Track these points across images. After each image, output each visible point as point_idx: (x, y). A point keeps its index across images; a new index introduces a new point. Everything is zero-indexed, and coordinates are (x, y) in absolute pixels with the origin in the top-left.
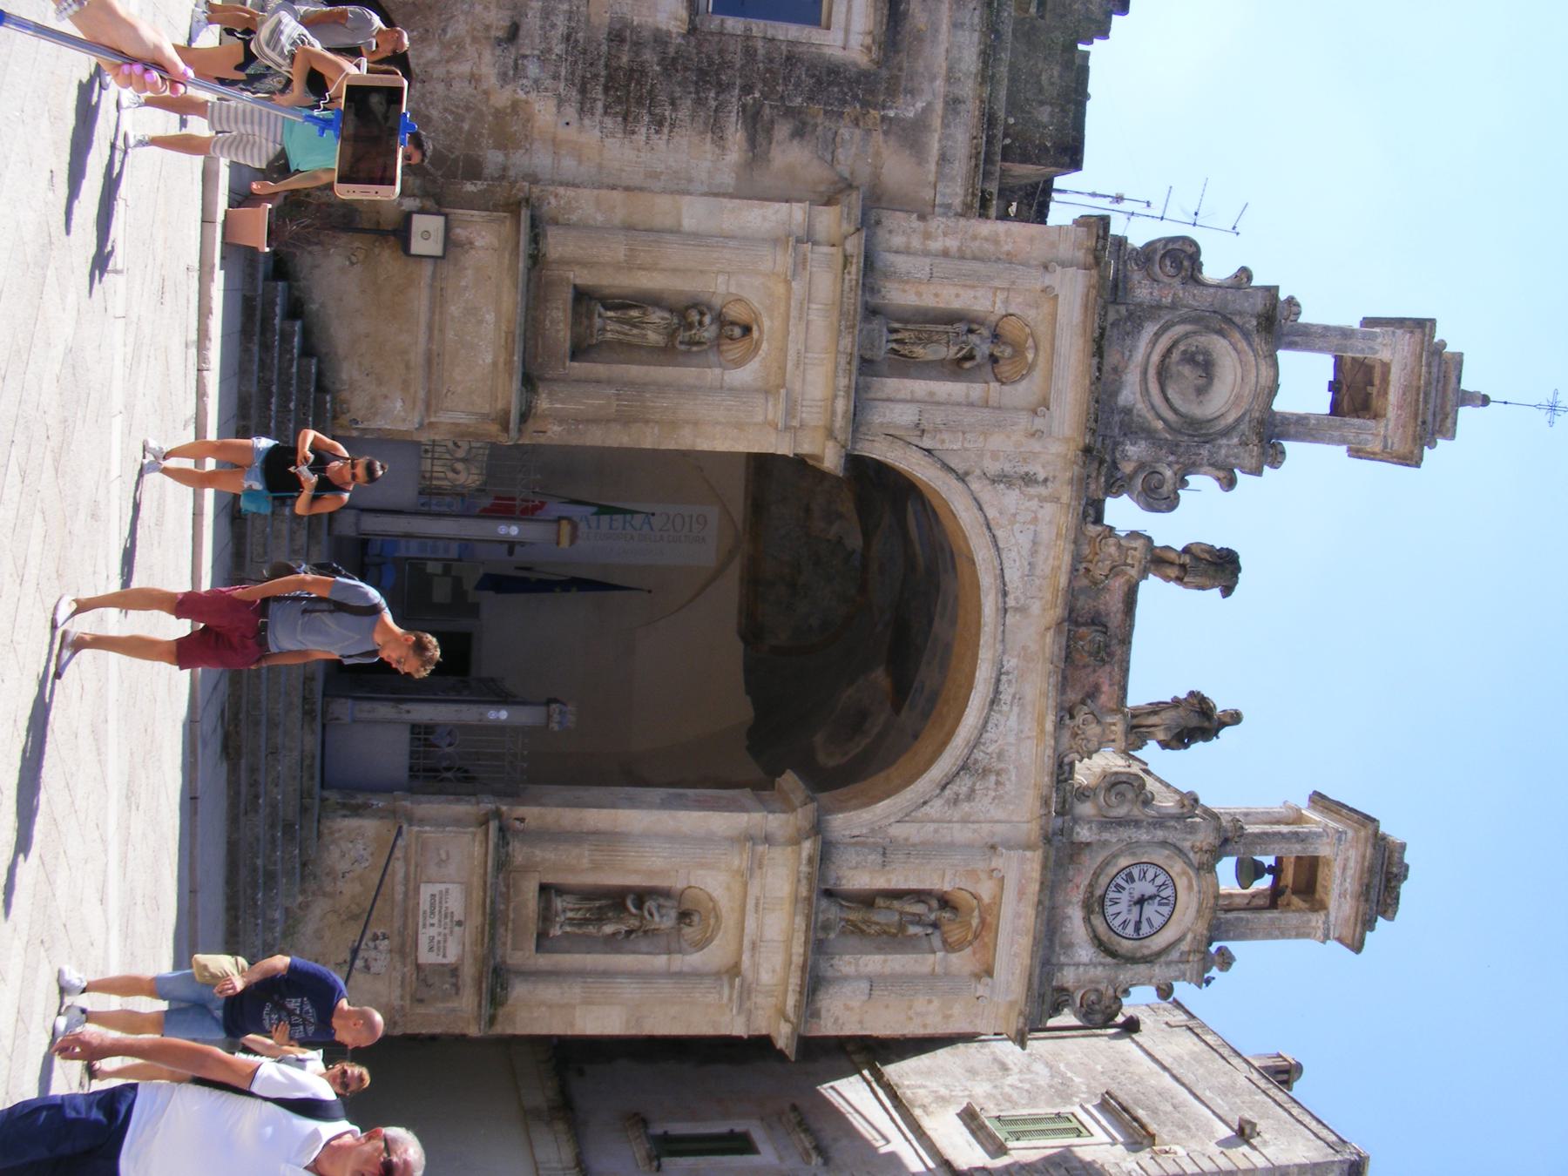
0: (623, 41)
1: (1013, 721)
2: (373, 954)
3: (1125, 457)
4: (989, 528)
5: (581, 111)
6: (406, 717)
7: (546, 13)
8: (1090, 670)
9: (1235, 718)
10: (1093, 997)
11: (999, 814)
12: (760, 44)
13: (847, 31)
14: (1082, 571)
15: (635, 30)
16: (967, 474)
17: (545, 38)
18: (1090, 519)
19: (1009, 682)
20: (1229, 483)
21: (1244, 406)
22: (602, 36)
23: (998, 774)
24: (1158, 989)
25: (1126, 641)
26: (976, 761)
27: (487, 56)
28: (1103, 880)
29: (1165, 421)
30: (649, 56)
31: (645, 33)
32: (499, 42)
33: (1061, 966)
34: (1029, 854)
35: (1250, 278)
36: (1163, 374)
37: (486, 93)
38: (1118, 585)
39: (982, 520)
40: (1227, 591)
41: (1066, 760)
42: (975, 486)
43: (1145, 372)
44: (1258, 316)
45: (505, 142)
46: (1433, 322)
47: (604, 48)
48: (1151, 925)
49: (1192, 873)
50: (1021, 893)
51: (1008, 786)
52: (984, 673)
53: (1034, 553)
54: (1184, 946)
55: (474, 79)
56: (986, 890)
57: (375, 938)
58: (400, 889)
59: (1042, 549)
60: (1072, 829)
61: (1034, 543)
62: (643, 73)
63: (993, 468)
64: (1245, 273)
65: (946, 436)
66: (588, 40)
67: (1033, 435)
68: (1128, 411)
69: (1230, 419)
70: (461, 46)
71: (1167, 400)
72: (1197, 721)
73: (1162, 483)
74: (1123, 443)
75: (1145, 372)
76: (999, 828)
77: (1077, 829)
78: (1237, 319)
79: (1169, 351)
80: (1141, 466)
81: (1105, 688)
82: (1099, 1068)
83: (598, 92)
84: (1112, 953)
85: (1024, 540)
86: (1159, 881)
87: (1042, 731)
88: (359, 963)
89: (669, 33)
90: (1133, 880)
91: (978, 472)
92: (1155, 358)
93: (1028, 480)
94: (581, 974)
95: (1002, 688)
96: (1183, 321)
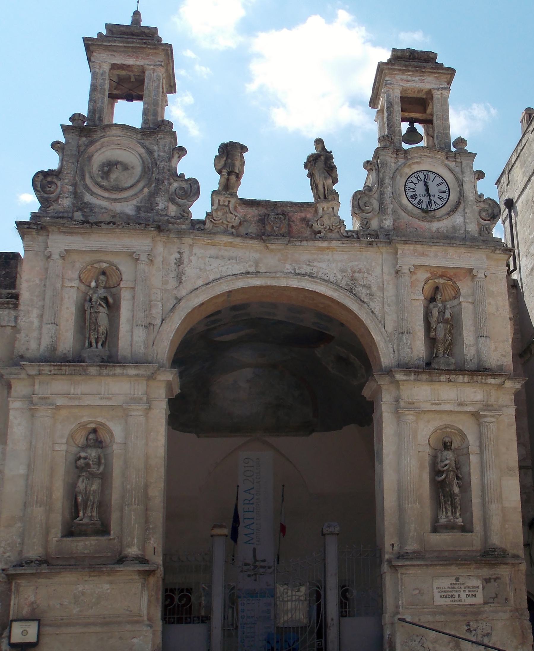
1: (323, 265)
2: (479, 631)
4: (208, 284)
6: (336, 621)
8: (291, 223)
10: (484, 214)
11: (378, 271)
14: (233, 230)
16: (176, 298)
18: (202, 226)
19: (299, 268)
24: (478, 179)
26: (347, 285)
28: (416, 211)
29: (144, 187)
33: (467, 232)
34: (400, 252)
36: (118, 189)
39: (203, 288)
41: (345, 234)
42: (183, 292)
48: (441, 184)
49: (410, 162)
51: (361, 266)
52: (294, 283)
57: (469, 630)
58: (438, 618)
60: (385, 230)
61: (217, 257)
63: (173, 283)
68: (138, 209)
73: (182, 188)
74: (157, 210)
75: (115, 200)
76: (386, 270)
80: (172, 200)
82: (531, 216)
84: (458, 203)
86: (415, 180)
87: (328, 248)
88: (486, 641)
90: (416, 195)
91: (175, 292)
93: (179, 262)
94: (484, 505)
95: (303, 272)
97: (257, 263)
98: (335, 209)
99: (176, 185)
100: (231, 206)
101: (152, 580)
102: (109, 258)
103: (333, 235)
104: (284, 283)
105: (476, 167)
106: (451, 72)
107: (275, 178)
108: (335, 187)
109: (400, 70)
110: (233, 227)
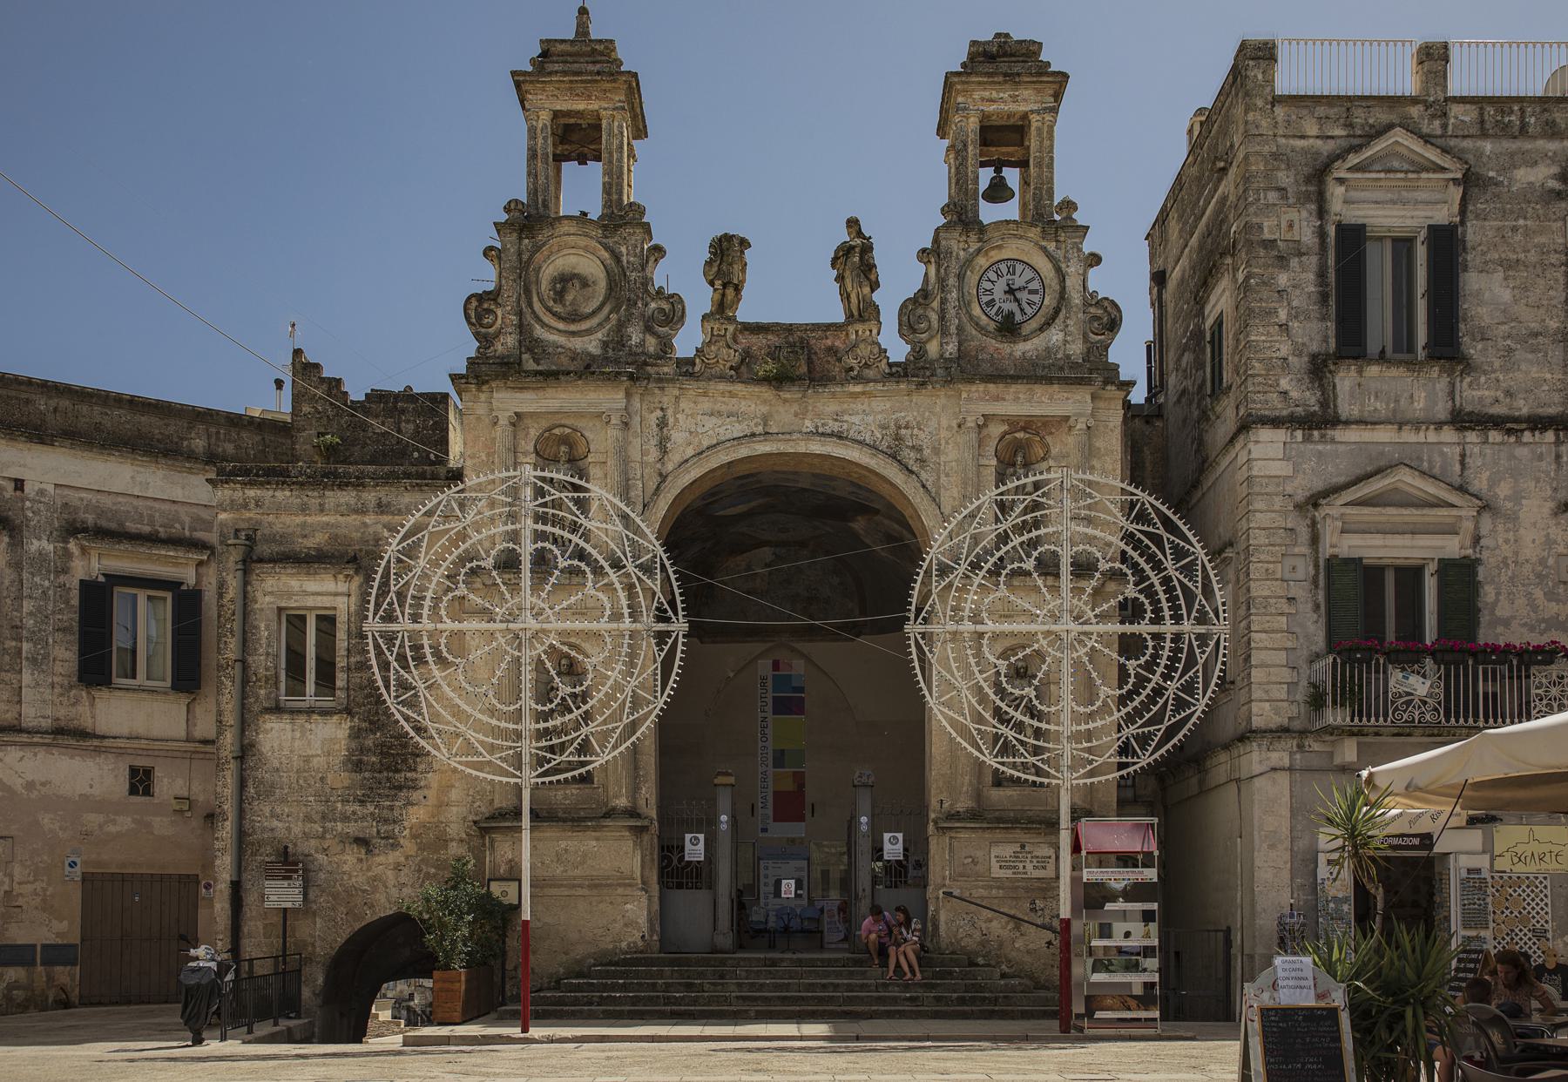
0: (360, 761)
1: (856, 419)
3: (642, 343)
5: (415, 788)
7: (345, 819)
9: (853, 224)
12: (353, 660)
13: (336, 594)
15: (351, 752)
17: (363, 818)
20: (658, 251)
21: (594, 243)
22: (359, 777)
23: (899, 428)
25: (789, 329)
27: (381, 859)
30: (369, 743)
31: (353, 745)
32: (369, 852)
34: (964, 395)
35: (491, 248)
36: (574, 317)
37: (407, 858)
38: (744, 340)
40: (744, 243)
42: (670, 467)
43: (573, 334)
44: (520, 239)
45: (443, 841)
46: (514, 73)
47: (367, 775)
50: (997, 398)
52: (816, 447)
53: (720, 414)
54: (1051, 246)
55: (398, 867)
56: (996, 430)
59: (717, 407)
62: (383, 745)
63: (654, 454)
64: (487, 252)
65: (632, 494)
66: (362, 786)
67: (626, 424)
68: (605, 345)
69: (606, 255)
70: (375, 878)
71: (594, 313)
72: (855, 260)
75: (573, 334)
76: (944, 423)
77: (947, 355)
78: (525, 257)
79: (554, 314)
81: (829, 342)
83: (400, 777)
85: (711, 422)
86: (993, 276)
87: (863, 393)
89: (351, 728)
92: (561, 326)
93: (662, 424)
96: (530, 305)
97: (765, 420)
98: (875, 331)
99: (653, 305)
100: (729, 336)
101: (646, 838)
102: (567, 422)
103: (870, 373)
104: (802, 448)
105: (1088, 247)
106: (1063, 77)
107: (792, 289)
108: (877, 297)
109: (979, 83)
110: (731, 368)
